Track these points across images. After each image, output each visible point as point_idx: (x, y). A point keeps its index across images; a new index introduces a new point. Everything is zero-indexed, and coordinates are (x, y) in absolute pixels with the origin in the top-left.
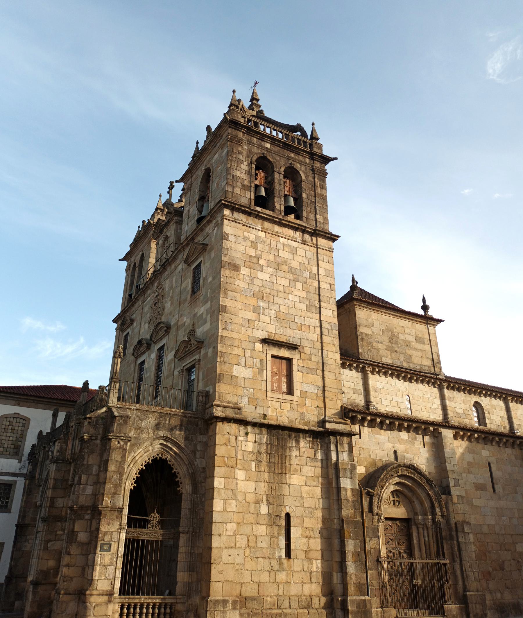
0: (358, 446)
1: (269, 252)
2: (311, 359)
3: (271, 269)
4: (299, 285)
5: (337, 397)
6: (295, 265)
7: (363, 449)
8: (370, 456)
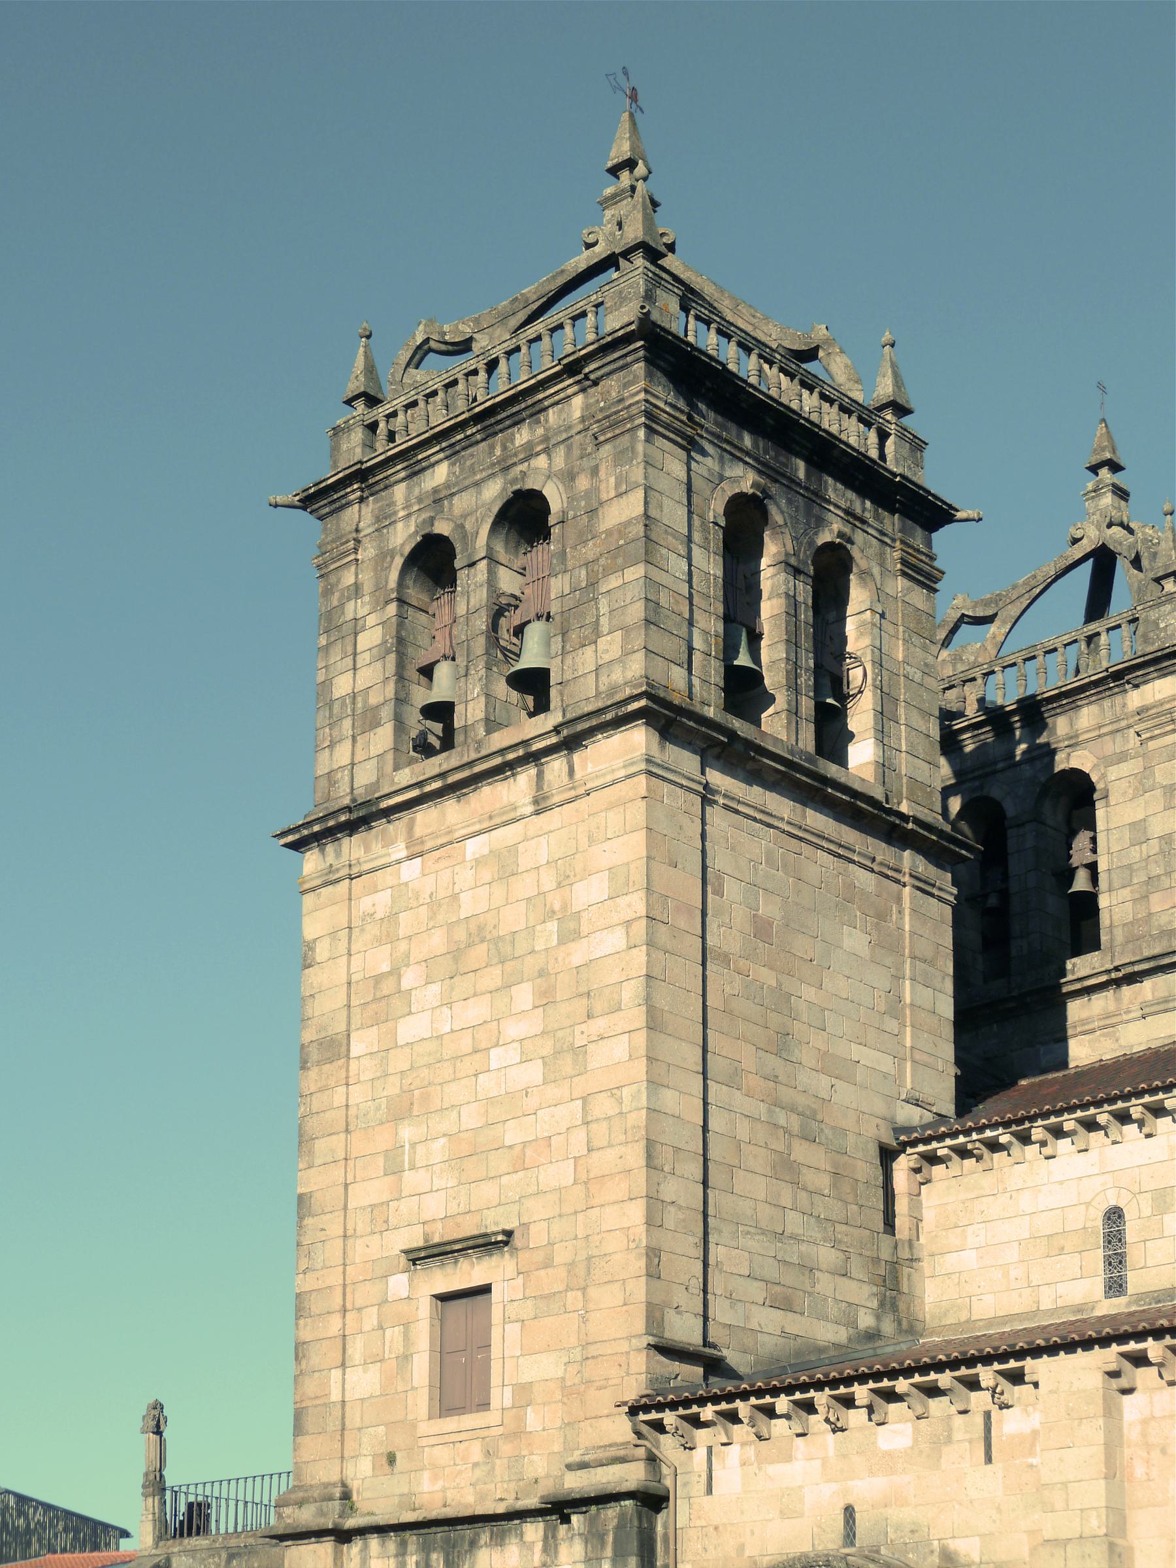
0: (699, 1523)
1: (431, 925)
2: (548, 1264)
3: (435, 988)
4: (524, 995)
5: (625, 1367)
6: (513, 919)
7: (716, 1528)
8: (741, 1548)
